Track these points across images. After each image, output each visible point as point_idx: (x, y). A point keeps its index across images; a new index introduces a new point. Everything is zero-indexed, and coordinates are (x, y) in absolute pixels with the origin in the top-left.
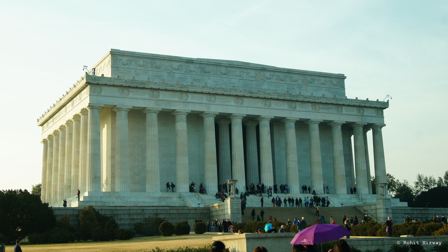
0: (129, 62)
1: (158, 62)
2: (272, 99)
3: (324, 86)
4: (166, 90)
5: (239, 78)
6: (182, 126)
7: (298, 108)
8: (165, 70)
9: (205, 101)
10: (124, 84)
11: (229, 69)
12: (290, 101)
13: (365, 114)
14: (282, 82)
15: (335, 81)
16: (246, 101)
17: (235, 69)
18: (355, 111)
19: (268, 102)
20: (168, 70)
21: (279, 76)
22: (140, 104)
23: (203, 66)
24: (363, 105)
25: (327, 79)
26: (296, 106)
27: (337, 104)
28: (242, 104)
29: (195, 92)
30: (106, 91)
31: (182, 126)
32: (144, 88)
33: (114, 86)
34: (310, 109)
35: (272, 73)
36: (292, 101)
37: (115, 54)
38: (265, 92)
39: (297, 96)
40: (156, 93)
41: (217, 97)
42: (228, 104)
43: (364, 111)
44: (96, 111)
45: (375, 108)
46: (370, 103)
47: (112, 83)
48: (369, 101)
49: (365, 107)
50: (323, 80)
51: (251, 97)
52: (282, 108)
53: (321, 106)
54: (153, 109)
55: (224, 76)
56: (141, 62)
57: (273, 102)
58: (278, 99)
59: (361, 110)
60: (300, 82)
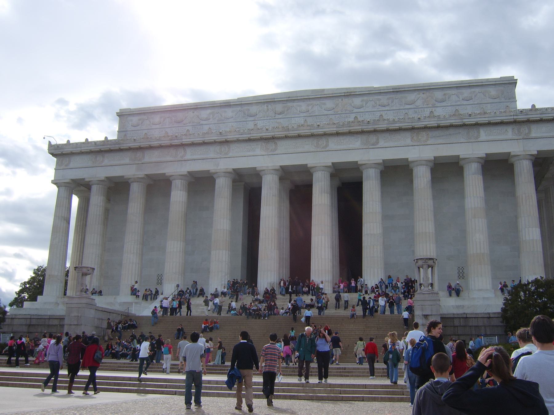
0: (140, 122)
1: (180, 115)
2: (325, 135)
3: (471, 102)
5: (305, 114)
6: (178, 196)
7: (382, 143)
8: (190, 123)
10: (93, 148)
11: (290, 104)
12: (362, 132)
14: (384, 109)
15: (493, 91)
17: (298, 104)
18: (509, 132)
19: (323, 142)
20: (193, 123)
21: (379, 100)
23: (246, 108)
25: (477, 90)
26: (378, 139)
27: (464, 126)
28: (275, 149)
29: (193, 144)
30: (76, 162)
31: (178, 196)
32: (121, 150)
33: (81, 153)
34: (408, 141)
35: (365, 98)
36: (369, 133)
38: (312, 125)
39: (375, 122)
40: (139, 154)
43: (530, 132)
44: (63, 189)
46: (538, 112)
47: (78, 150)
48: (537, 109)
49: (529, 122)
50: (466, 93)
51: (286, 137)
52: (351, 146)
53: (431, 133)
54: (132, 177)
55: (280, 116)
58: (338, 134)
59: (524, 129)
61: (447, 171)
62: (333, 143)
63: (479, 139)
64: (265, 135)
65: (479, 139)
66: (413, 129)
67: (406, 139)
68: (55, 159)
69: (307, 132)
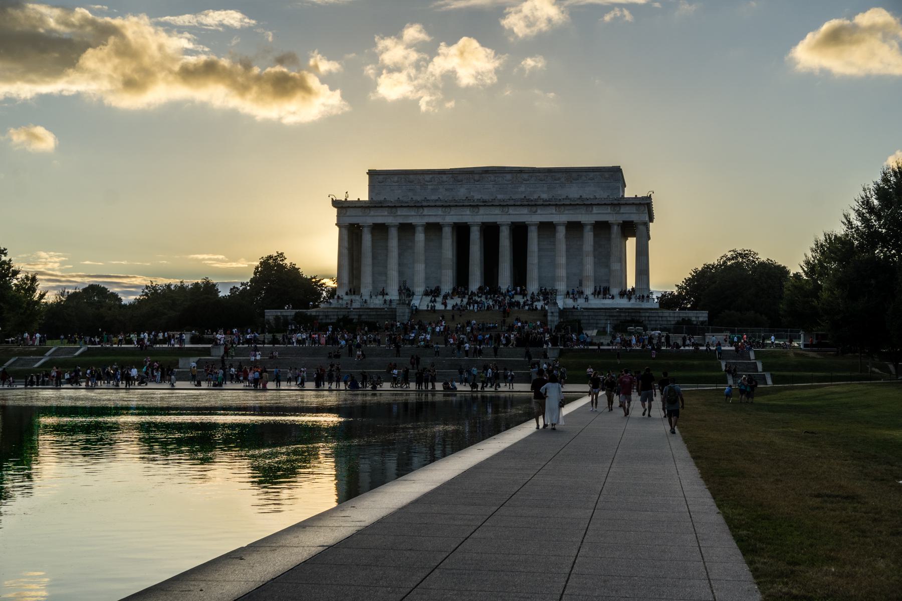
4: (402, 206)
6: (420, 237)
7: (539, 212)
16: (482, 210)
18: (609, 210)
19: (506, 209)
22: (380, 220)
27: (584, 205)
29: (429, 206)
30: (350, 212)
31: (420, 237)
34: (554, 211)
36: (532, 205)
37: (373, 175)
40: (394, 210)
49: (619, 204)
50: (591, 175)
60: (563, 180)
61: (574, 228)
62: (511, 210)
67: (553, 210)
68: (336, 210)
69: (497, 204)
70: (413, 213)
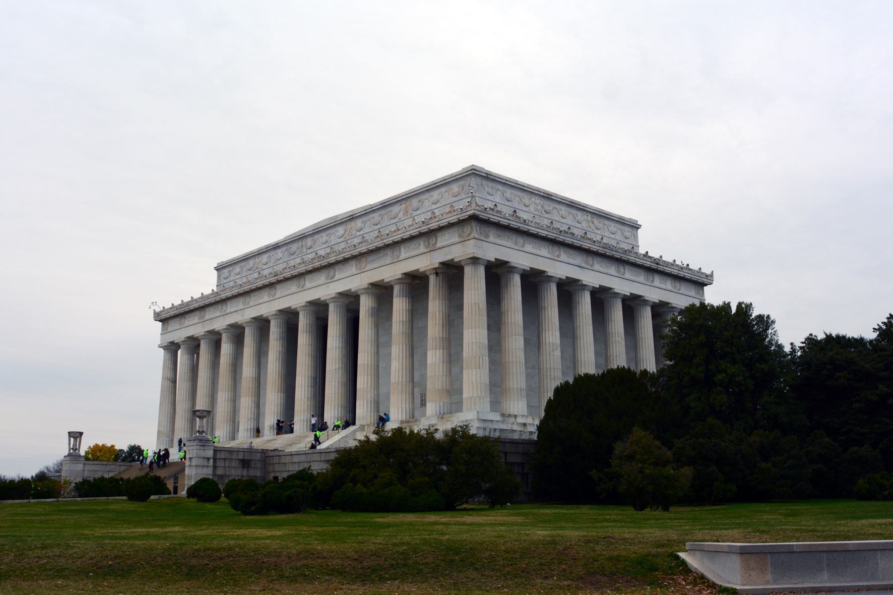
3: (438, 205)
7: (337, 276)
9: (241, 306)
11: (316, 237)
13: (439, 245)
14: (377, 227)
16: (280, 291)
18: (421, 246)
24: (424, 229)
25: (443, 189)
27: (387, 246)
28: (274, 295)
30: (173, 325)
31: (226, 348)
35: (364, 219)
41: (252, 294)
42: (261, 301)
43: (436, 243)
45: (450, 225)
46: (437, 219)
50: (435, 195)
56: (237, 269)
57: (308, 277)
62: (309, 282)
63: (402, 257)
64: (266, 282)
65: (401, 258)
66: (354, 257)
67: (352, 268)
70: (218, 314)
